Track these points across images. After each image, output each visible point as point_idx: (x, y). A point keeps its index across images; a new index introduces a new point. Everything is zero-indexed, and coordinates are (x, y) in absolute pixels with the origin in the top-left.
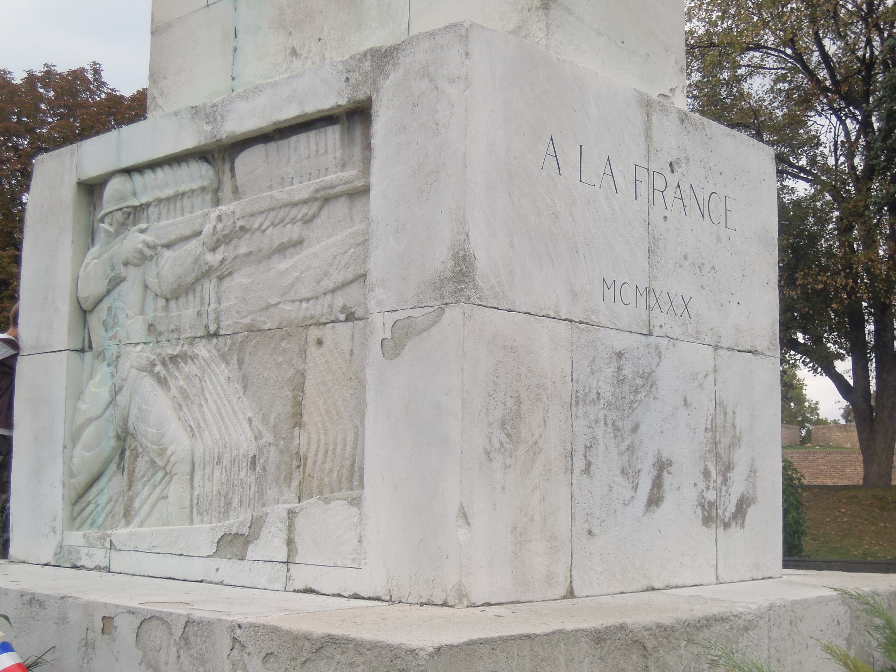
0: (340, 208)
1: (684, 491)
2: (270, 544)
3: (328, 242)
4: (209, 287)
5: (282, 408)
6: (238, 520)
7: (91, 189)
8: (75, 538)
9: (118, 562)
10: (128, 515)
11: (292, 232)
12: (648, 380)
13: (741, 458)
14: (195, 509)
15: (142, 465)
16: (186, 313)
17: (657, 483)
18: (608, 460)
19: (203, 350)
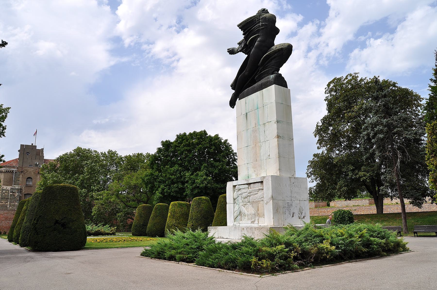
0: (261, 191)
1: (296, 216)
2: (256, 222)
3: (260, 193)
4: (248, 197)
5: (257, 209)
6: (253, 220)
7: (234, 186)
8: (235, 223)
9: (241, 225)
10: (241, 220)
11: (257, 192)
12: (292, 205)
13: (304, 212)
14: (248, 219)
15: (242, 215)
16: (246, 200)
17: (293, 215)
18: (287, 213)
19: (248, 203)
